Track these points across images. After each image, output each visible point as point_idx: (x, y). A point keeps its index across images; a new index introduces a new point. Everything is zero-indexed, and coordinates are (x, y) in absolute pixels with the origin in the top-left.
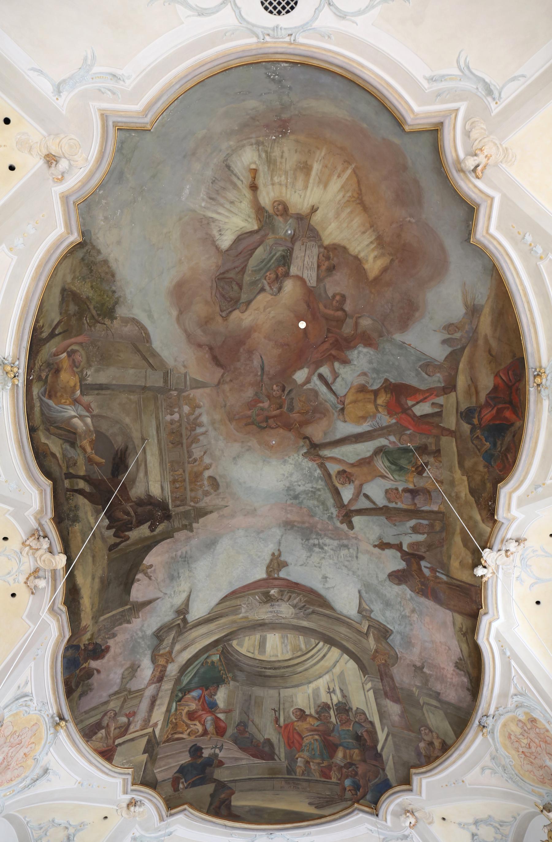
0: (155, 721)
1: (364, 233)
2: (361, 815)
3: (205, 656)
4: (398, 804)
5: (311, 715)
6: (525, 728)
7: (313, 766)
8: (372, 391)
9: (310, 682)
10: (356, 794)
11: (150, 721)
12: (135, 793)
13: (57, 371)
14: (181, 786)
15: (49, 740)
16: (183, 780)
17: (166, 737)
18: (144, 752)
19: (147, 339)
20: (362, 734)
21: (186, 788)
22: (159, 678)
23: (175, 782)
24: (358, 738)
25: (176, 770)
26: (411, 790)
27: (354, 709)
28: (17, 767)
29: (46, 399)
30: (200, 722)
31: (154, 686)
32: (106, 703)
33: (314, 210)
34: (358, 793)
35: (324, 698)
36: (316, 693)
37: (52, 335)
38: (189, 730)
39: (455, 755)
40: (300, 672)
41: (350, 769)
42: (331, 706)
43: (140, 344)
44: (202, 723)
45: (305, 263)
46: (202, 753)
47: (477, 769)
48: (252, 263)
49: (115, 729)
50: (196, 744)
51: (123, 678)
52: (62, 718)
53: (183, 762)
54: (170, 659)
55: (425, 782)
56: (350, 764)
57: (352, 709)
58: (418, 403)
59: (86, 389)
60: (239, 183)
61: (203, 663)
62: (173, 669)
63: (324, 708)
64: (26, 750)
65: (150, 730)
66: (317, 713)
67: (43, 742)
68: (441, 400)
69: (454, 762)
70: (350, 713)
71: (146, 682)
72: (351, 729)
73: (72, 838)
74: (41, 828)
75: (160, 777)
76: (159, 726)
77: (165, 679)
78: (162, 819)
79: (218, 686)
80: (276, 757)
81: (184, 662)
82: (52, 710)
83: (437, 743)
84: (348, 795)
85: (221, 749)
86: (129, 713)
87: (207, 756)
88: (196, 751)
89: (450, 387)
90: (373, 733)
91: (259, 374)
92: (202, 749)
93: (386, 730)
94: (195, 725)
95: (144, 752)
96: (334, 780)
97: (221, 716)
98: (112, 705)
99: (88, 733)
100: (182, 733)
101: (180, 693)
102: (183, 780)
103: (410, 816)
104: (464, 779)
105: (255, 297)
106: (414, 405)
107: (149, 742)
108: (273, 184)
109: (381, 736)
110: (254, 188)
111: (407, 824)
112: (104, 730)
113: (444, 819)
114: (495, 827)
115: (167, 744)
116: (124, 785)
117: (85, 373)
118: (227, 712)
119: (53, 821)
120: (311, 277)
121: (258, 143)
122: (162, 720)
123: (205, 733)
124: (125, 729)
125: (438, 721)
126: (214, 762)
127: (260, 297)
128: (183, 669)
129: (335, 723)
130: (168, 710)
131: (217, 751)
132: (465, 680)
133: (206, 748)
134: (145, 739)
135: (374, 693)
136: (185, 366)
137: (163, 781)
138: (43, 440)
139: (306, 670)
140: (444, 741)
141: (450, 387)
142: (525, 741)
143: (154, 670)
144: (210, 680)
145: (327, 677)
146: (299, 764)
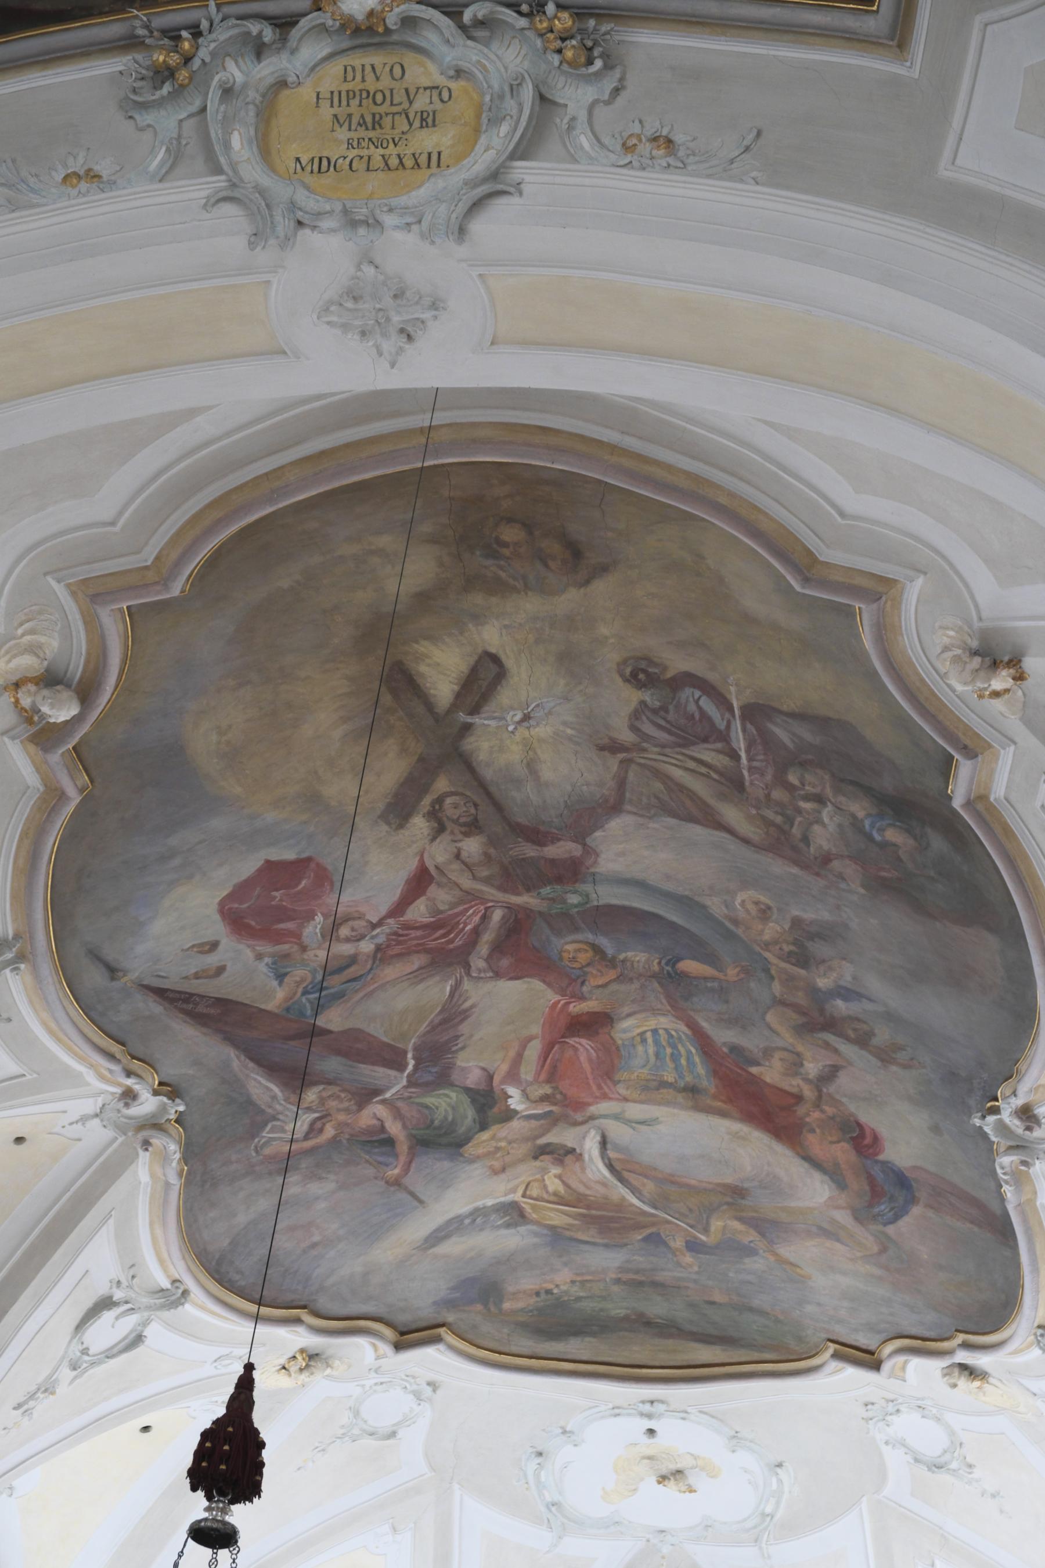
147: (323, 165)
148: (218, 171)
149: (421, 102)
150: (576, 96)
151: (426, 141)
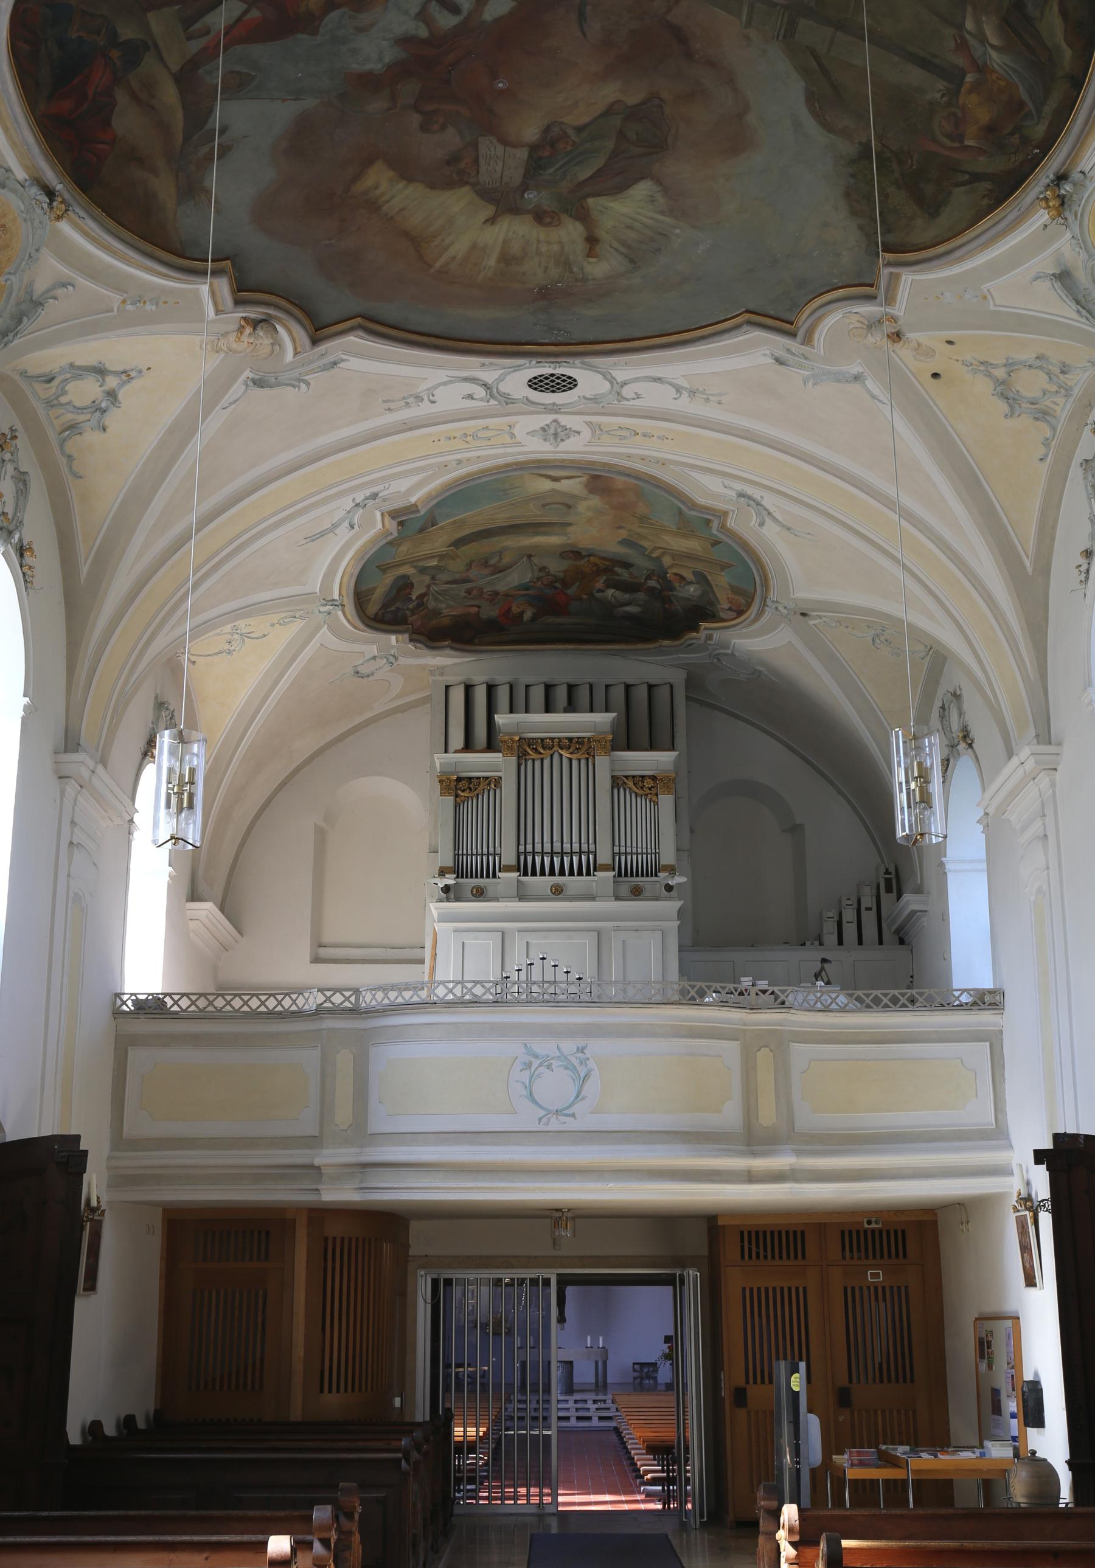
1: (402, 210)
8: (340, 6)
13: (990, 129)
19: (811, 99)
29: (1031, 106)
33: (492, 220)
37: (976, 178)
43: (828, 96)
45: (501, 163)
48: (598, 162)
58: (239, 20)
59: (954, 77)
60: (616, 244)
68: (194, 47)
89: (187, 77)
91: (589, 8)
105: (595, 120)
106: (246, 12)
108: (560, 242)
110: (592, 241)
117: (945, 99)
120: (489, 147)
121: (585, 280)
127: (586, 119)
136: (747, 38)
138: (1068, 53)
141: (187, 77)
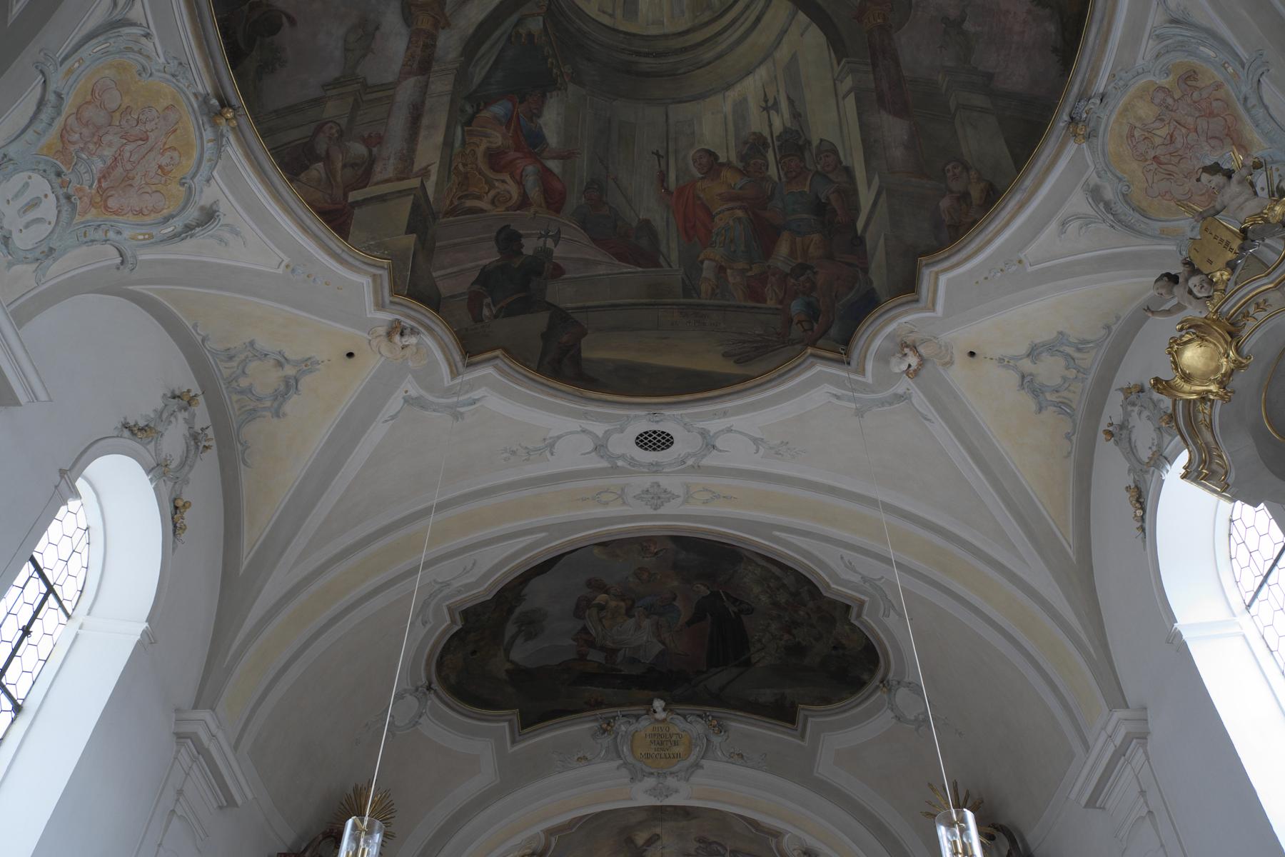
0: (424, 165)
2: (820, 368)
3: (514, 18)
4: (890, 337)
5: (728, 165)
6: (1170, 101)
7: (732, 277)
9: (729, 87)
10: (812, 329)
11: (413, 163)
12: (399, 308)
14: (486, 312)
15: (206, 156)
16: (489, 300)
17: (448, 202)
18: (410, 230)
20: (828, 198)
21: (496, 317)
22: (423, 63)
23: (474, 302)
24: (820, 208)
25: (473, 279)
26: (917, 301)
27: (815, 142)
28: (148, 189)
30: (512, 177)
31: (412, 81)
32: (318, 102)
34: (816, 326)
35: (756, 122)
36: (741, 108)
38: (492, 193)
39: (1012, 204)
40: (709, 63)
41: (802, 278)
42: (769, 140)
44: (518, 178)
46: (522, 246)
47: (1053, 226)
49: (344, 166)
50: (508, 226)
51: (346, 50)
52: (224, 103)
53: (486, 262)
54: (442, 22)
55: (944, 280)
56: (804, 268)
57: (810, 143)
61: (510, 36)
62: (449, 44)
63: (756, 145)
64: (164, 160)
65: (415, 183)
66: (742, 158)
67: (196, 155)
69: (1007, 224)
70: (807, 155)
71: (397, 67)
72: (807, 189)
73: (292, 382)
74: (231, 358)
75: (445, 288)
76: (433, 178)
77: (435, 67)
78: (455, 373)
79: (544, 96)
80: (662, 260)
81: (471, 31)
82: (204, 85)
83: (976, 193)
84: (796, 331)
85: (557, 238)
86: (370, 136)
87: (531, 253)
88: (509, 240)
90: (849, 194)
92: (520, 236)
93: (876, 181)
94: (503, 181)
95: (410, 230)
96: (771, 303)
97: (554, 165)
98: (331, 110)
99: (293, 161)
100: (479, 198)
101: (469, 106)
102: (489, 300)
103: (910, 353)
104: (1022, 256)
107: (415, 208)
109: (866, 197)
111: (904, 367)
112: (321, 164)
113: (972, 354)
114: (1068, 357)
115: (451, 218)
116: (375, 292)
118: (566, 156)
119: (252, 343)
122: (437, 165)
123: (524, 202)
124: (364, 172)
125: (981, 142)
126: (542, 269)
128: (472, 46)
129: (776, 179)
130: (448, 143)
131: (550, 243)
132: (1051, 28)
133: (529, 236)
134: (408, 202)
135: (858, 100)
137: (451, 297)
139: (720, 56)
140: (991, 185)
142: (1164, 132)
143: (410, 41)
144: (529, 80)
145: (762, 72)
146: (704, 274)
147: (648, 756)
148: (620, 757)
149: (674, 738)
150: (716, 740)
151: (676, 750)
